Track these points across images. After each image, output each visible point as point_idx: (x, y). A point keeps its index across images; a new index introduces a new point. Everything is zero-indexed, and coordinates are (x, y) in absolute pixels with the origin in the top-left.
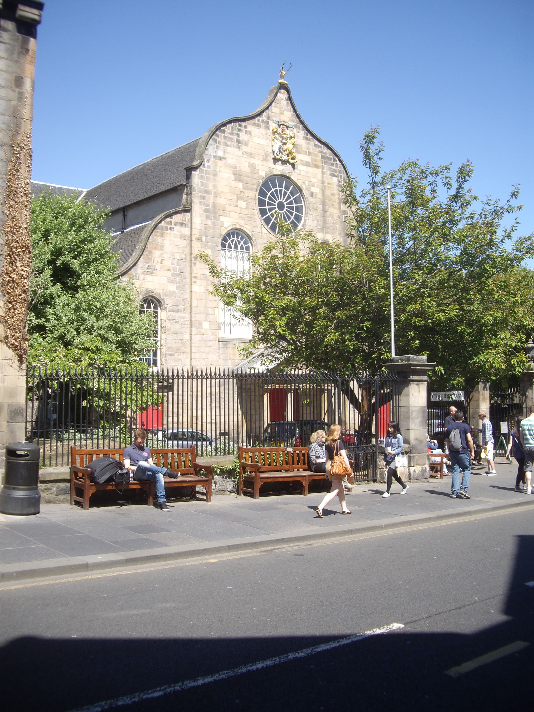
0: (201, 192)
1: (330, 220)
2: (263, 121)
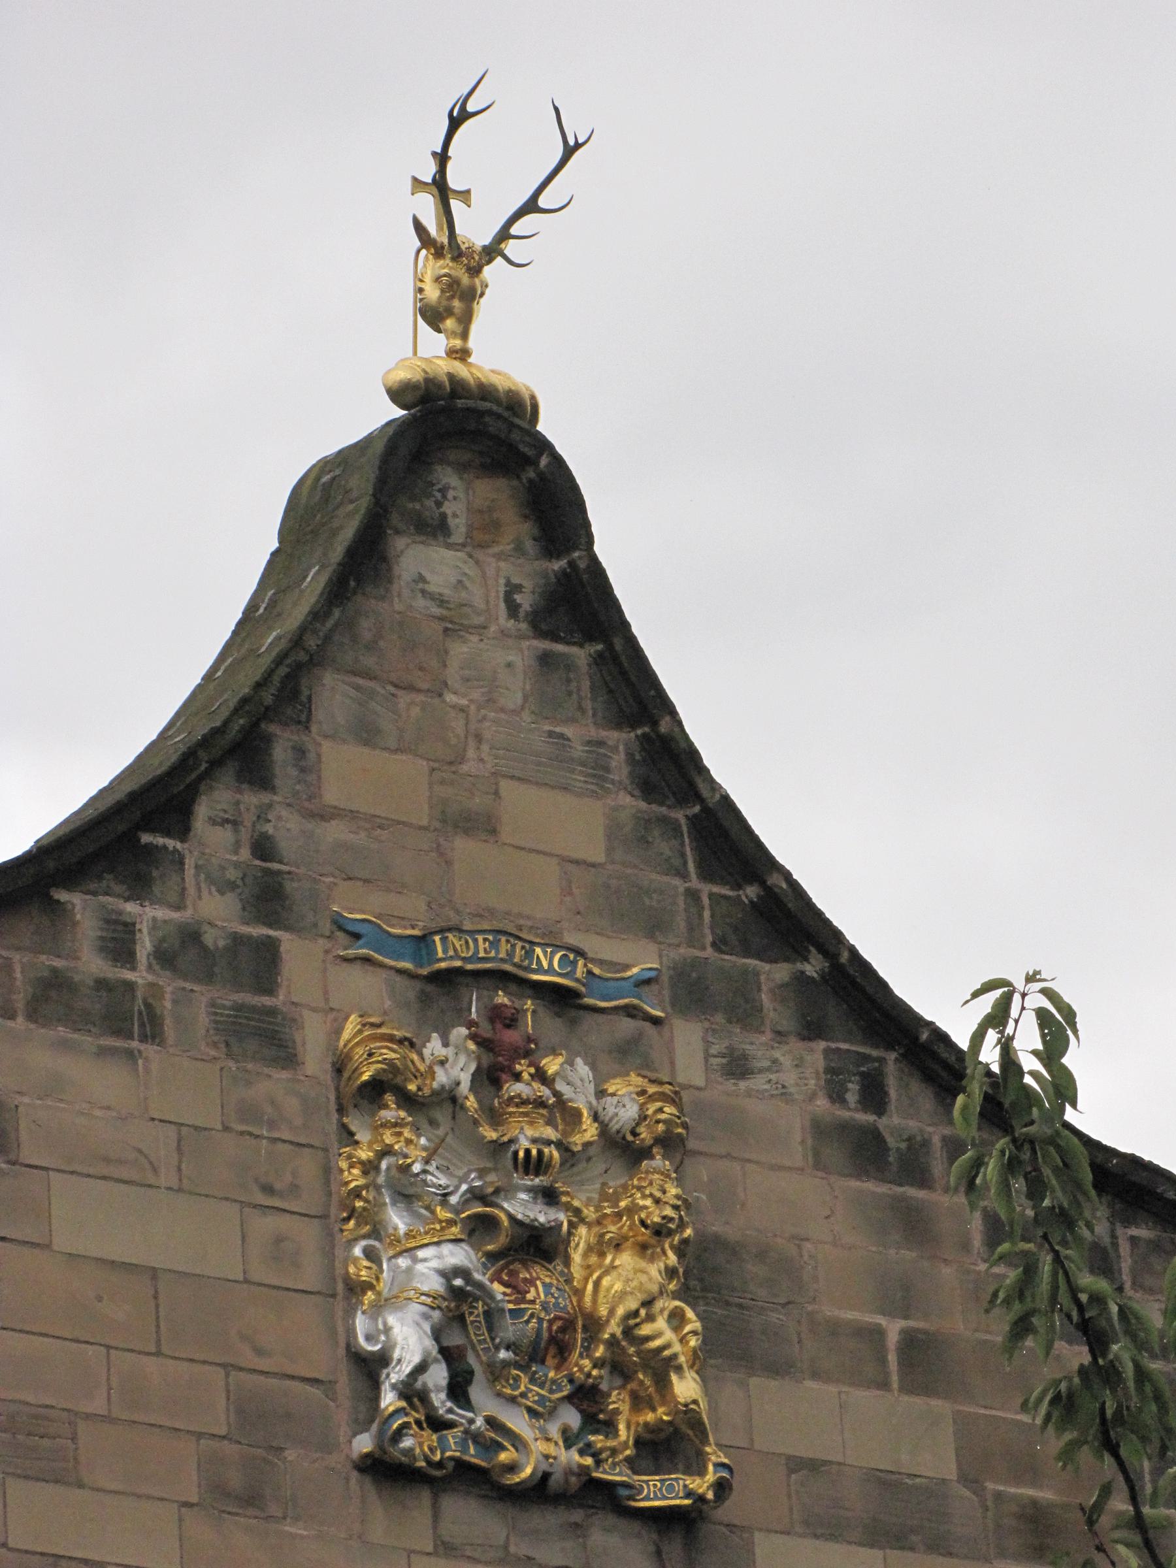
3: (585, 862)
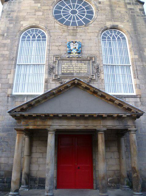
0: (7, 12)
1: (117, 15)
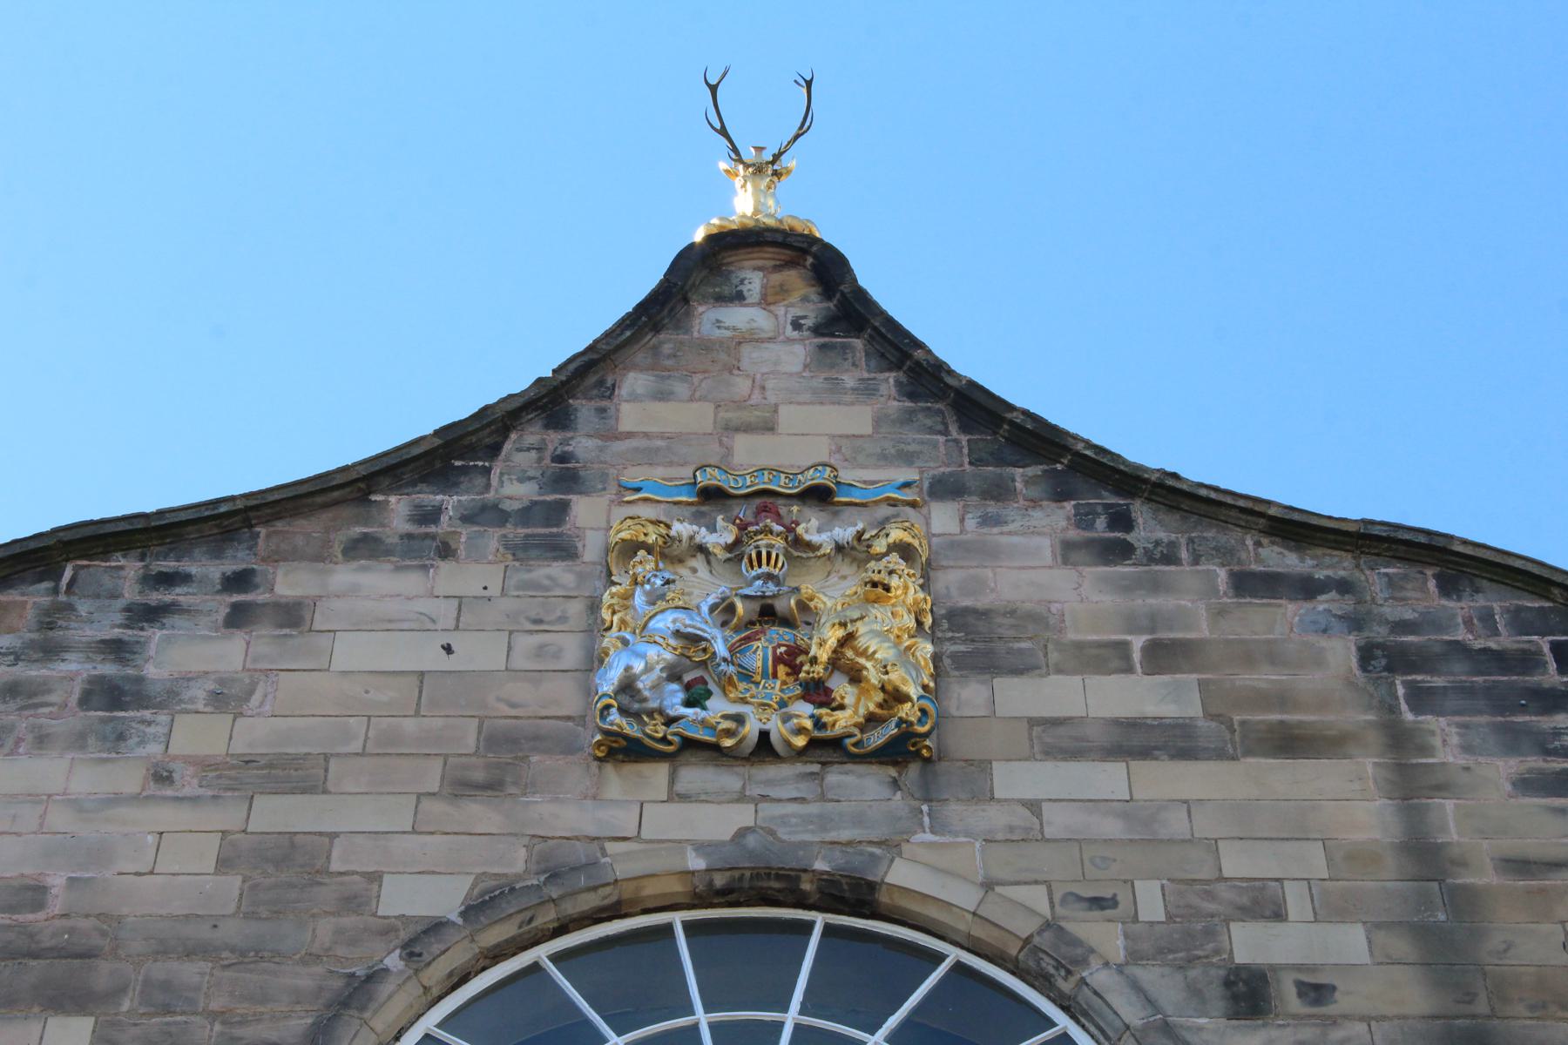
2: (487, 514)
3: (854, 436)
